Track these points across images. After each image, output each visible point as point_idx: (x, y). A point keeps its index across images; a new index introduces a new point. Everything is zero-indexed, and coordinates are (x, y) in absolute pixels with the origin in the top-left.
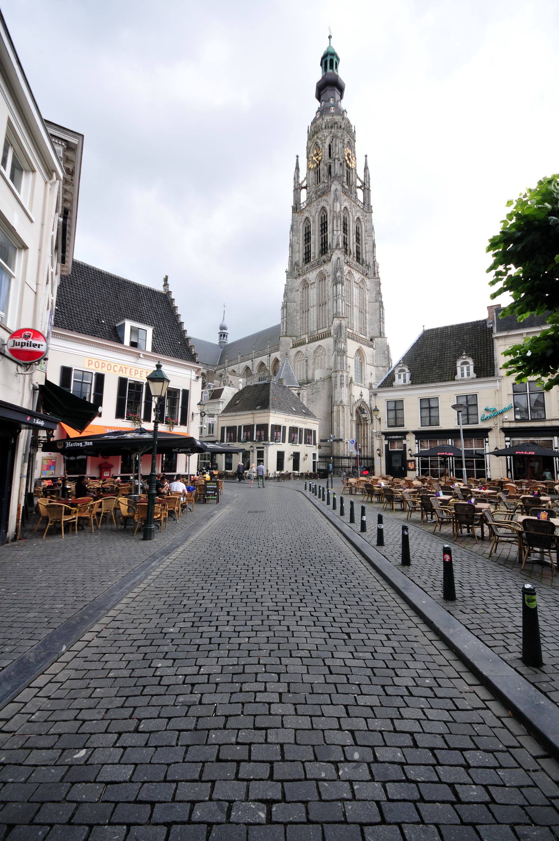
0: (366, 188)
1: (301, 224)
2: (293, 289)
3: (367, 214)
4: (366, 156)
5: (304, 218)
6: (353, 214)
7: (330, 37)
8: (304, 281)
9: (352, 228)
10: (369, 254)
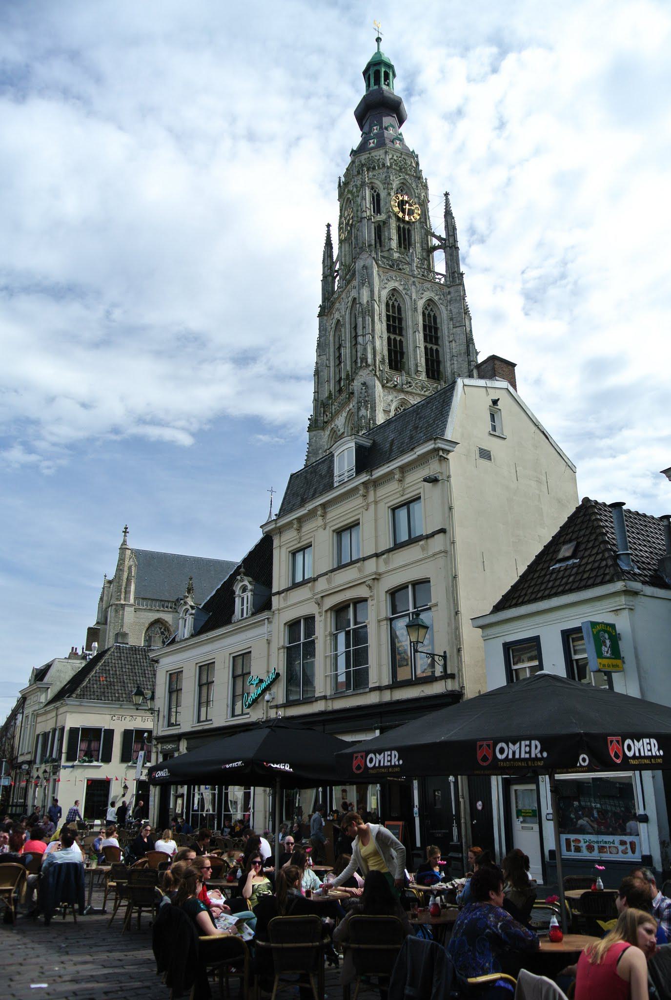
0: (450, 245)
1: (332, 333)
2: (318, 450)
3: (452, 290)
4: (447, 194)
5: (334, 321)
6: (414, 297)
7: (378, 40)
8: (334, 431)
9: (415, 324)
10: (460, 360)
